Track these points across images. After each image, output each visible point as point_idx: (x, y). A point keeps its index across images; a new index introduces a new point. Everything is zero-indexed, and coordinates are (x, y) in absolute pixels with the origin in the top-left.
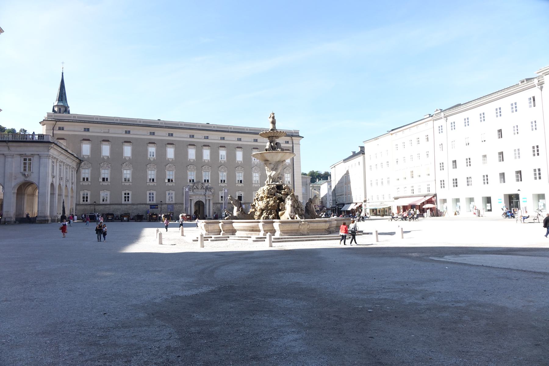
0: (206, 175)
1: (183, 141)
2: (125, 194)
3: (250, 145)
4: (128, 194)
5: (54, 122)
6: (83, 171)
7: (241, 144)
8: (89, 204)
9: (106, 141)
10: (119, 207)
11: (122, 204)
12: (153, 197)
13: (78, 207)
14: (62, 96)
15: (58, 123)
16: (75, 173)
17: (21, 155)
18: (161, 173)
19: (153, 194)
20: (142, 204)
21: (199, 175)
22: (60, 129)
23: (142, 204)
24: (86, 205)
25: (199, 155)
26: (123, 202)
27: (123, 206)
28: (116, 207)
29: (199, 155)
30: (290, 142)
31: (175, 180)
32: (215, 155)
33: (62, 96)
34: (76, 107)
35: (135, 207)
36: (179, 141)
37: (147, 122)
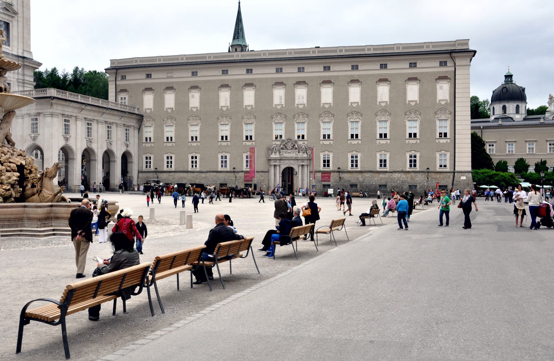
0: (301, 129)
1: (267, 79)
2: (192, 158)
3: (373, 75)
4: (196, 158)
5: (115, 71)
6: (145, 129)
7: (359, 75)
8: (152, 172)
9: (170, 88)
10: (185, 175)
11: (188, 172)
12: (226, 162)
13: (140, 175)
14: (239, 32)
15: (119, 71)
16: (136, 132)
17: (29, 115)
18: (236, 129)
19: (226, 157)
20: (213, 172)
21: (290, 130)
22: (124, 78)
23: (213, 172)
24: (149, 172)
25: (290, 97)
26: (190, 169)
27: (190, 174)
28: (182, 175)
29: (290, 97)
30: (448, 64)
31: (255, 138)
32: (314, 96)
33: (239, 32)
34: (255, 43)
35: (203, 175)
36: (260, 80)
37: (196, 58)
